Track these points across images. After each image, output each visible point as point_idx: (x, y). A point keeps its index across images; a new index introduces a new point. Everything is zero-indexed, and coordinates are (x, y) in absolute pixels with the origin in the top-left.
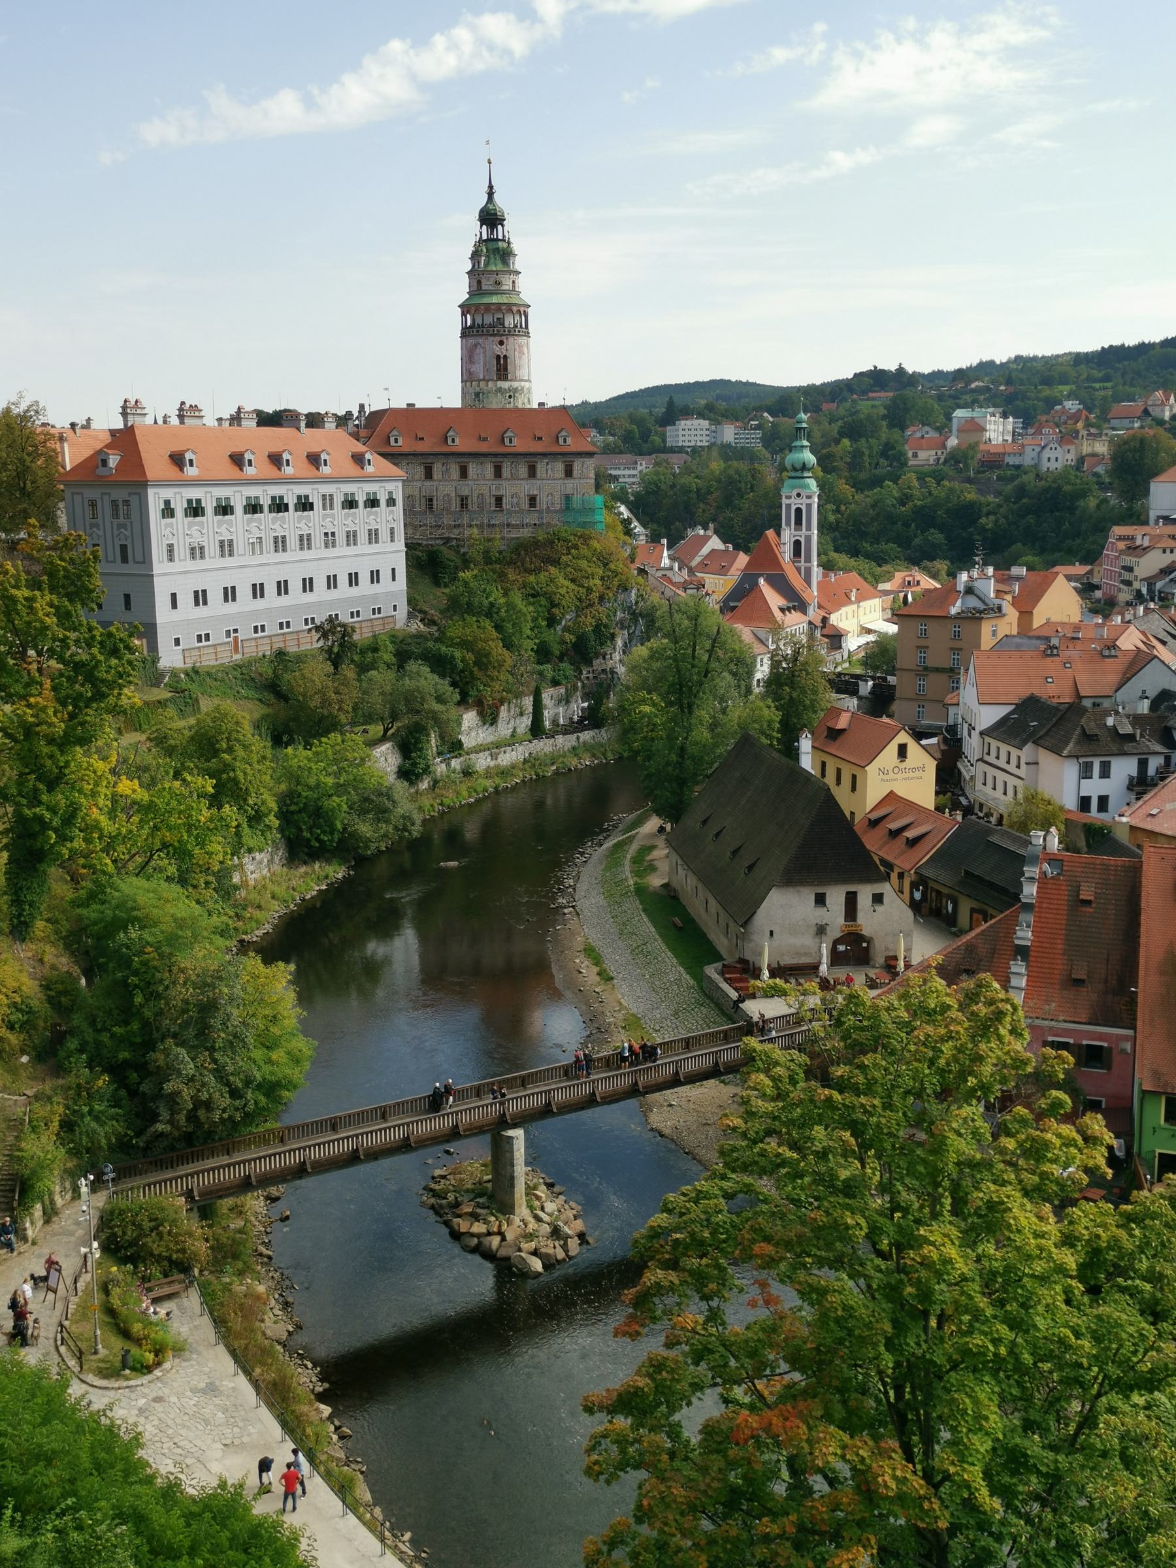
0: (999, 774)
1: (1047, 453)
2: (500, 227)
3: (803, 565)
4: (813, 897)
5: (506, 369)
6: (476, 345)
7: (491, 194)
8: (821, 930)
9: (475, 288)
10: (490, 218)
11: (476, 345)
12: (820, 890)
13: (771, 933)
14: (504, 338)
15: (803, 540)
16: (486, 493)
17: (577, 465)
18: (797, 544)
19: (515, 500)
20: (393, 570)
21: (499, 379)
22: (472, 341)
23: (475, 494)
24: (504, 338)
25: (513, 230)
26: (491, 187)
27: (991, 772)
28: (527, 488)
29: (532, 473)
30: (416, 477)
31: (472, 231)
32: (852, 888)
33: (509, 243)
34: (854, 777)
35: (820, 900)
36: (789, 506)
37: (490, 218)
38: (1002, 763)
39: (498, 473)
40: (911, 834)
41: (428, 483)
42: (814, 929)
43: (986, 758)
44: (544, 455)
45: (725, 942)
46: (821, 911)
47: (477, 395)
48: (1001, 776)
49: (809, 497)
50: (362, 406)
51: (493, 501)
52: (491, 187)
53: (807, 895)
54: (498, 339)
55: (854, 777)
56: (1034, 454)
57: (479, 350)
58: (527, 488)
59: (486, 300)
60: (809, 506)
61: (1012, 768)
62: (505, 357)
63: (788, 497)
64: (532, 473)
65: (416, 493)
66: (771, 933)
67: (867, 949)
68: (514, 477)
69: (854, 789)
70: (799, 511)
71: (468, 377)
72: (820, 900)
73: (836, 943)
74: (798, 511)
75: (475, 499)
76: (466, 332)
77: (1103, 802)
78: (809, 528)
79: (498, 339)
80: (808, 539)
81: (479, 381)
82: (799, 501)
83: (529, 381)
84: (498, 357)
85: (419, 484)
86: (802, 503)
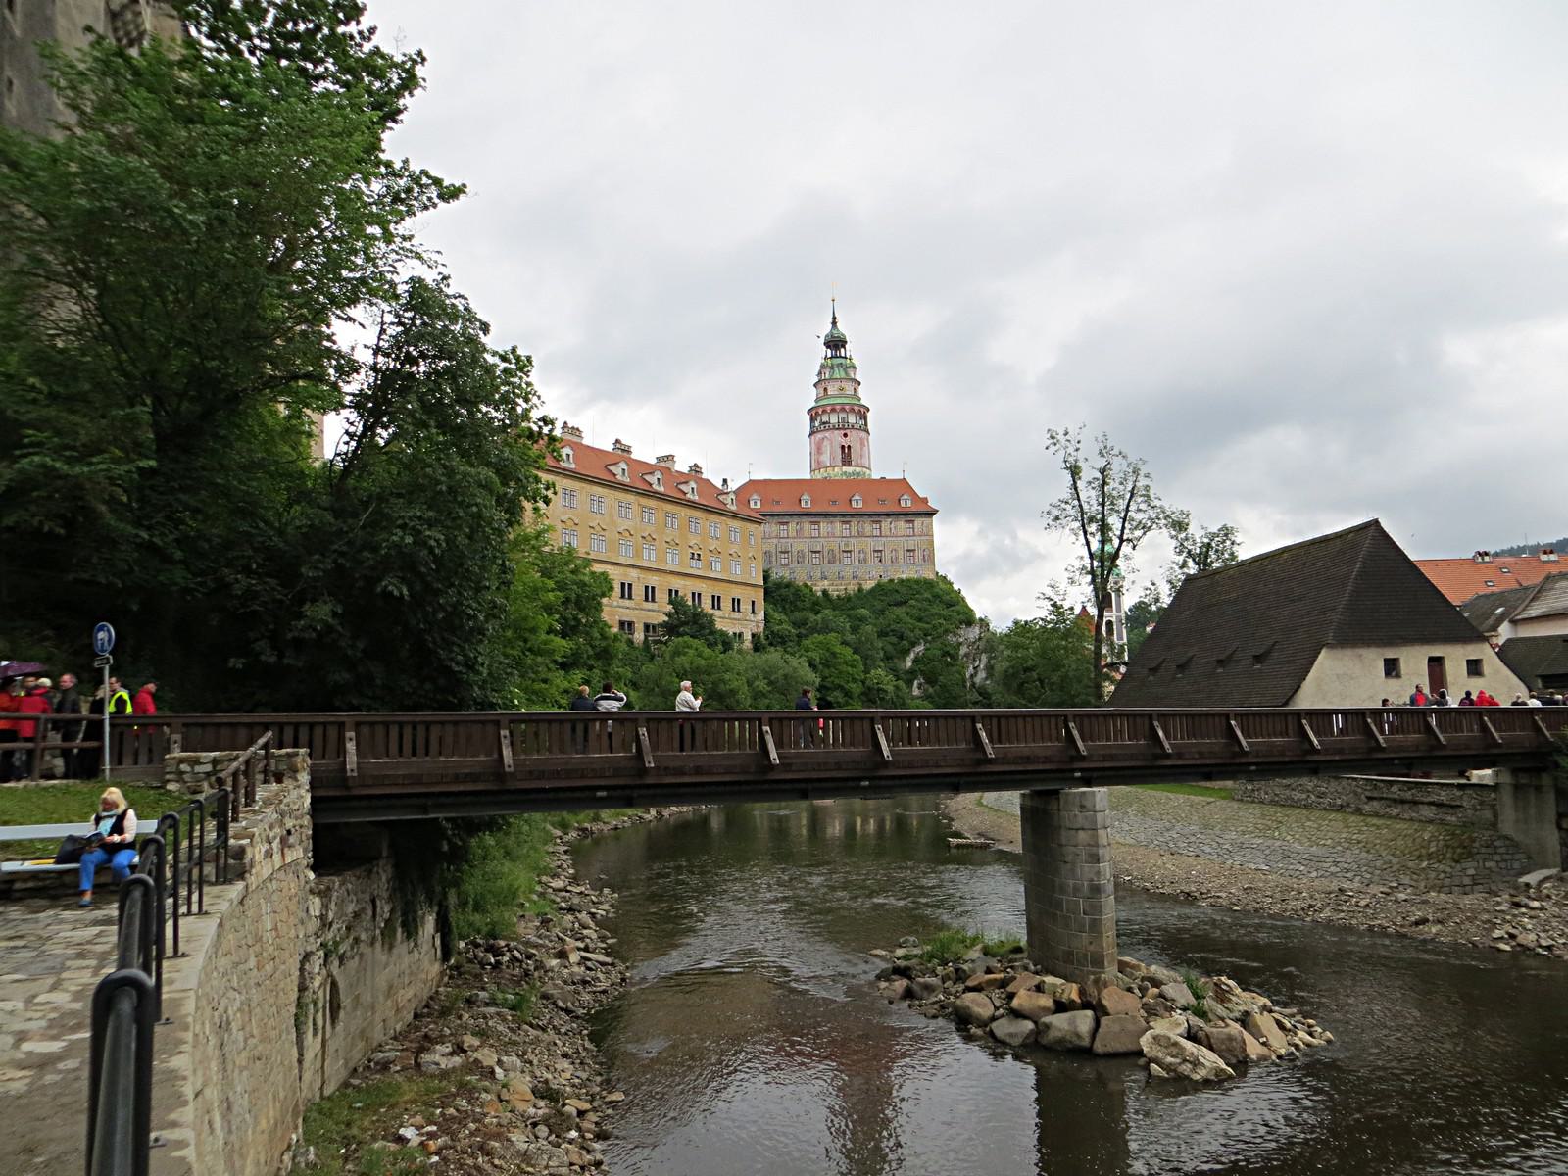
2: (842, 350)
4: (1381, 664)
7: (834, 323)
10: (835, 343)
12: (1391, 654)
14: (848, 432)
20: (753, 602)
21: (844, 465)
24: (848, 432)
26: (834, 318)
32: (1437, 651)
35: (1392, 668)
37: (835, 343)
44: (888, 515)
52: (834, 318)
53: (1374, 659)
54: (843, 432)
57: (826, 443)
62: (849, 447)
72: (1392, 668)
75: (826, 554)
79: (843, 432)
83: (869, 469)
84: (843, 447)
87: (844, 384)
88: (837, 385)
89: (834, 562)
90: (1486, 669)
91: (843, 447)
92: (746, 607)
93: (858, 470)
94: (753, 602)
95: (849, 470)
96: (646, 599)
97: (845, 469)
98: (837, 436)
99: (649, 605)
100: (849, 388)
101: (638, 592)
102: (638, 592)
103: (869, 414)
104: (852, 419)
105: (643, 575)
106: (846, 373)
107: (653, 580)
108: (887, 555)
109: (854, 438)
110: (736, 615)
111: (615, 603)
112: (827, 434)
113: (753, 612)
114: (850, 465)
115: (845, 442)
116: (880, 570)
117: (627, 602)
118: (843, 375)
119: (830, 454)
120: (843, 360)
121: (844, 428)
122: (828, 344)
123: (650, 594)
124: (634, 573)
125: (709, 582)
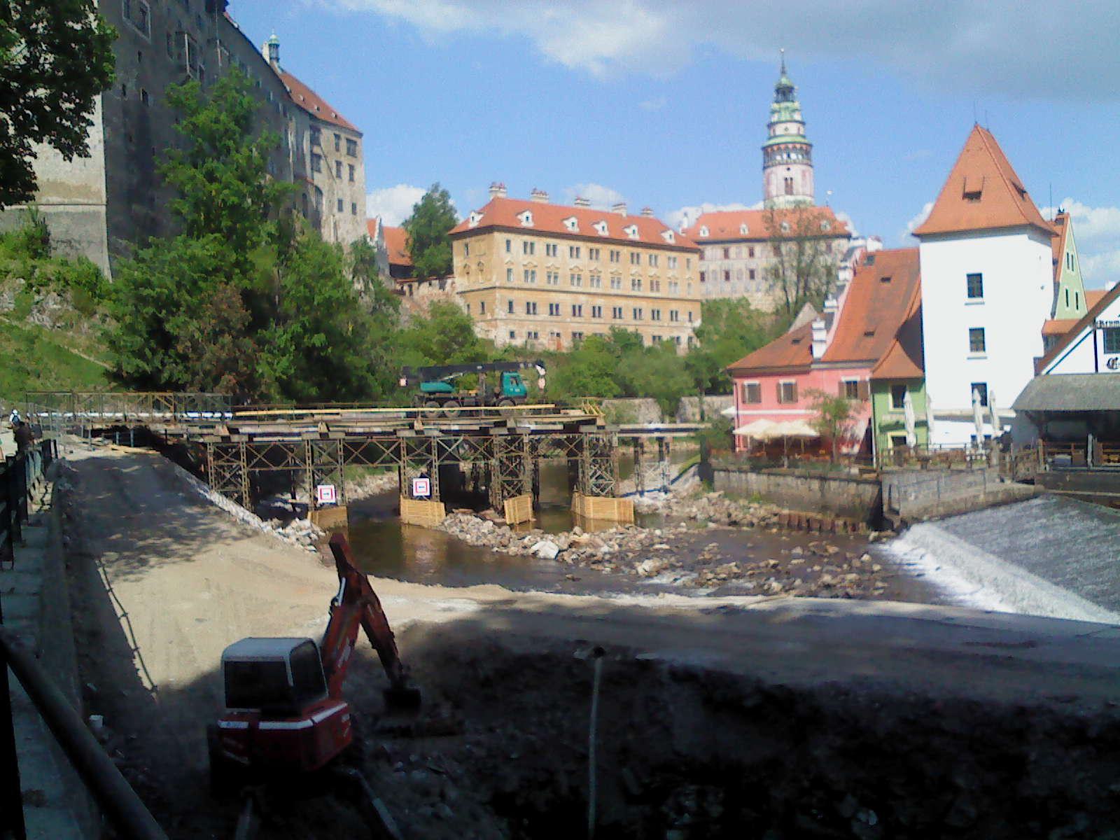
14: (790, 166)
20: (690, 313)
24: (790, 166)
41: (726, 261)
62: (791, 179)
65: (718, 269)
84: (786, 179)
85: (720, 263)
87: (789, 125)
91: (786, 179)
92: (683, 317)
93: (800, 198)
94: (690, 313)
96: (594, 316)
99: (597, 320)
101: (586, 311)
102: (586, 311)
105: (590, 299)
107: (599, 302)
110: (674, 324)
111: (568, 320)
113: (690, 321)
115: (788, 175)
117: (577, 319)
118: (788, 118)
123: (596, 312)
124: (583, 298)
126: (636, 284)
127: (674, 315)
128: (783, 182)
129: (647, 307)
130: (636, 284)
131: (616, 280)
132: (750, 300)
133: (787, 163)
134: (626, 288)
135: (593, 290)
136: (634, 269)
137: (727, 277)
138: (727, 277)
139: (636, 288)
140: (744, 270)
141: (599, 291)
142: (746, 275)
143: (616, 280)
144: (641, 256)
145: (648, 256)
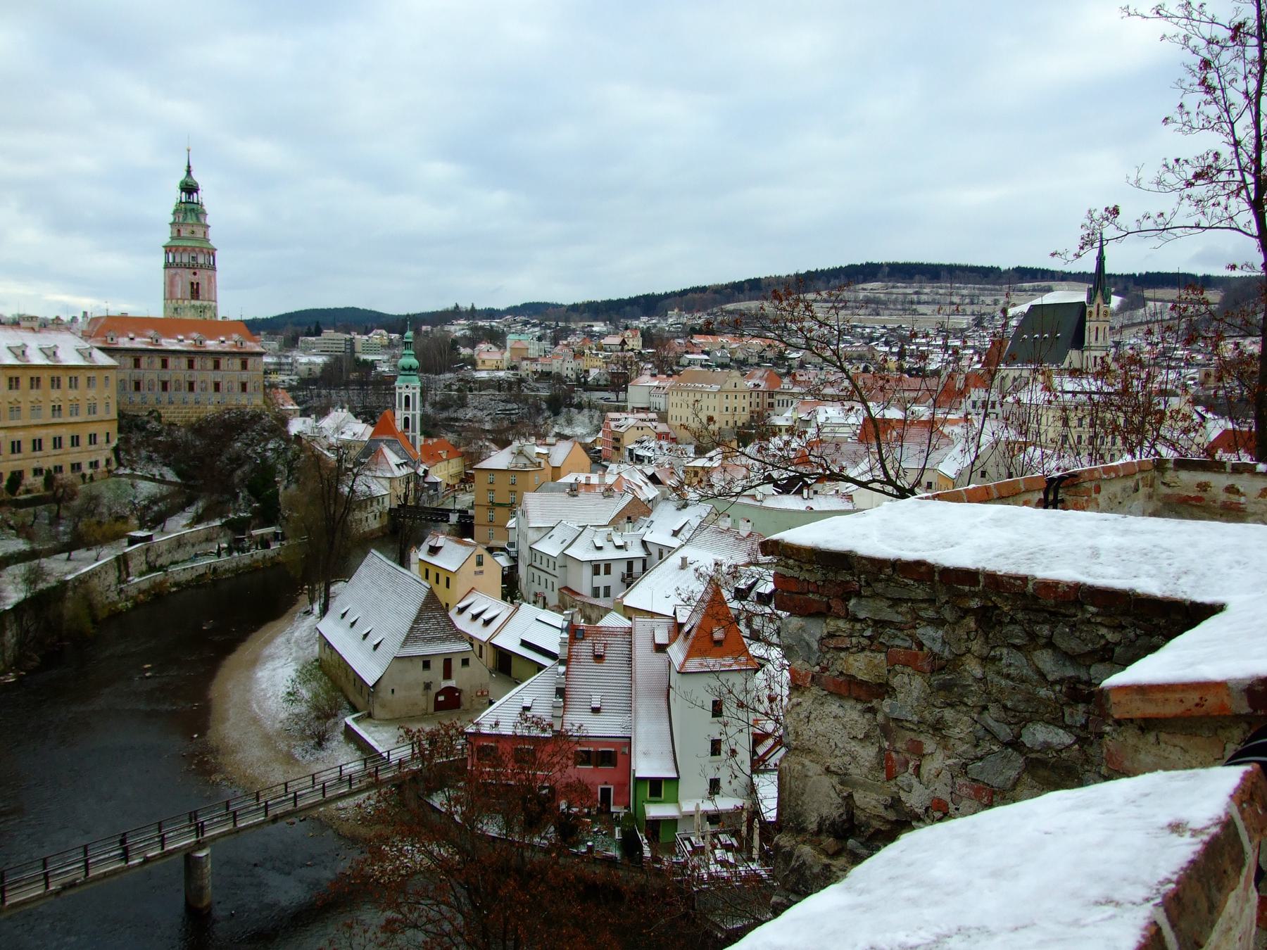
0: (543, 574)
1: (566, 365)
3: (410, 434)
5: (198, 292)
6: (176, 274)
7: (189, 172)
8: (428, 686)
9: (175, 235)
10: (189, 188)
11: (176, 274)
13: (393, 691)
14: (196, 271)
15: (410, 417)
16: (182, 379)
17: (251, 361)
18: (407, 420)
19: (204, 385)
20: (108, 434)
21: (192, 298)
22: (173, 271)
23: (174, 379)
25: (205, 196)
26: (189, 167)
27: (537, 573)
28: (212, 376)
29: (217, 366)
30: (128, 366)
31: (174, 195)
33: (202, 205)
34: (448, 579)
36: (400, 394)
37: (189, 188)
38: (544, 567)
39: (191, 365)
40: (486, 616)
41: (137, 371)
42: (422, 687)
43: (537, 564)
44: (226, 353)
45: (360, 699)
46: (427, 673)
47: (176, 309)
48: (543, 576)
49: (414, 388)
50: (85, 313)
51: (187, 385)
52: (189, 167)
55: (448, 579)
56: (558, 365)
57: (178, 278)
58: (212, 376)
59: (185, 243)
60: (414, 395)
61: (550, 570)
62: (198, 284)
63: (400, 388)
64: (217, 366)
65: (127, 378)
66: (393, 691)
67: (459, 696)
68: (203, 369)
69: (448, 586)
70: (407, 398)
71: (170, 295)
73: (438, 694)
74: (407, 398)
76: (167, 266)
77: (607, 589)
78: (414, 409)
79: (192, 271)
80: (414, 416)
81: (178, 299)
82: (407, 390)
83: (215, 301)
85: (129, 371)
86: (409, 392)
87: (195, 229)
88: (190, 229)
89: (180, 390)
90: (470, 663)
91: (192, 284)
92: (101, 439)
93: (205, 303)
94: (108, 434)
95: (197, 303)
97: (193, 302)
98: (187, 276)
99: (17, 456)
100: (200, 234)
103: (216, 253)
104: (201, 260)
106: (198, 218)
107: (18, 435)
108: (224, 386)
109: (202, 277)
112: (179, 271)
114: (197, 298)
115: (195, 279)
116: (216, 397)
119: (182, 288)
120: (195, 206)
121: (194, 267)
122: (183, 189)
125: (69, 426)
126: (57, 410)
127: (93, 439)
128: (189, 287)
129: (66, 434)
130: (57, 410)
131: (36, 408)
132: (162, 411)
133: (193, 268)
134: (47, 416)
135: (12, 423)
136: (55, 394)
137: (137, 386)
138: (137, 386)
139: (57, 412)
140: (156, 379)
141: (19, 423)
142: (158, 387)
143: (36, 408)
144: (62, 379)
145: (68, 379)
